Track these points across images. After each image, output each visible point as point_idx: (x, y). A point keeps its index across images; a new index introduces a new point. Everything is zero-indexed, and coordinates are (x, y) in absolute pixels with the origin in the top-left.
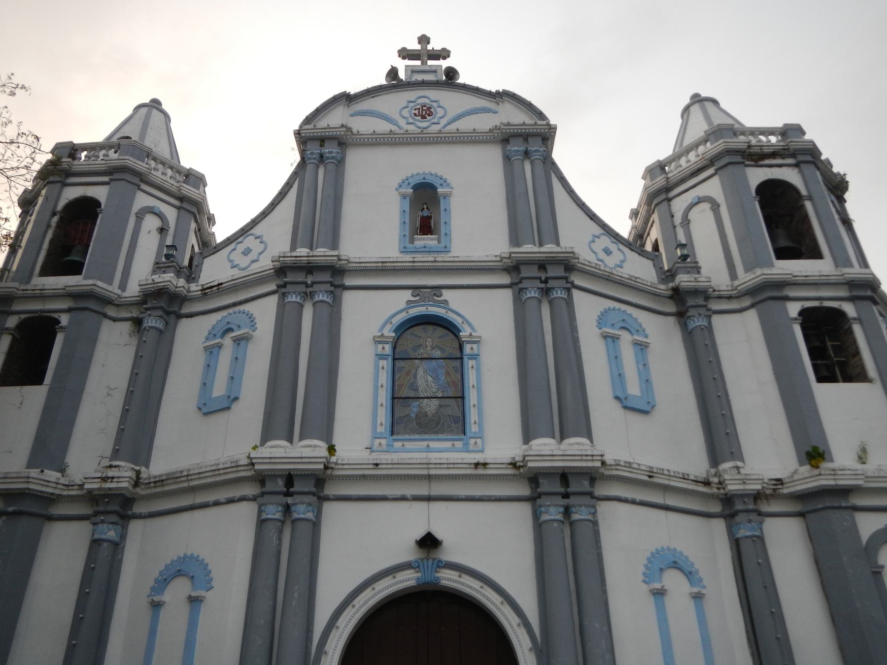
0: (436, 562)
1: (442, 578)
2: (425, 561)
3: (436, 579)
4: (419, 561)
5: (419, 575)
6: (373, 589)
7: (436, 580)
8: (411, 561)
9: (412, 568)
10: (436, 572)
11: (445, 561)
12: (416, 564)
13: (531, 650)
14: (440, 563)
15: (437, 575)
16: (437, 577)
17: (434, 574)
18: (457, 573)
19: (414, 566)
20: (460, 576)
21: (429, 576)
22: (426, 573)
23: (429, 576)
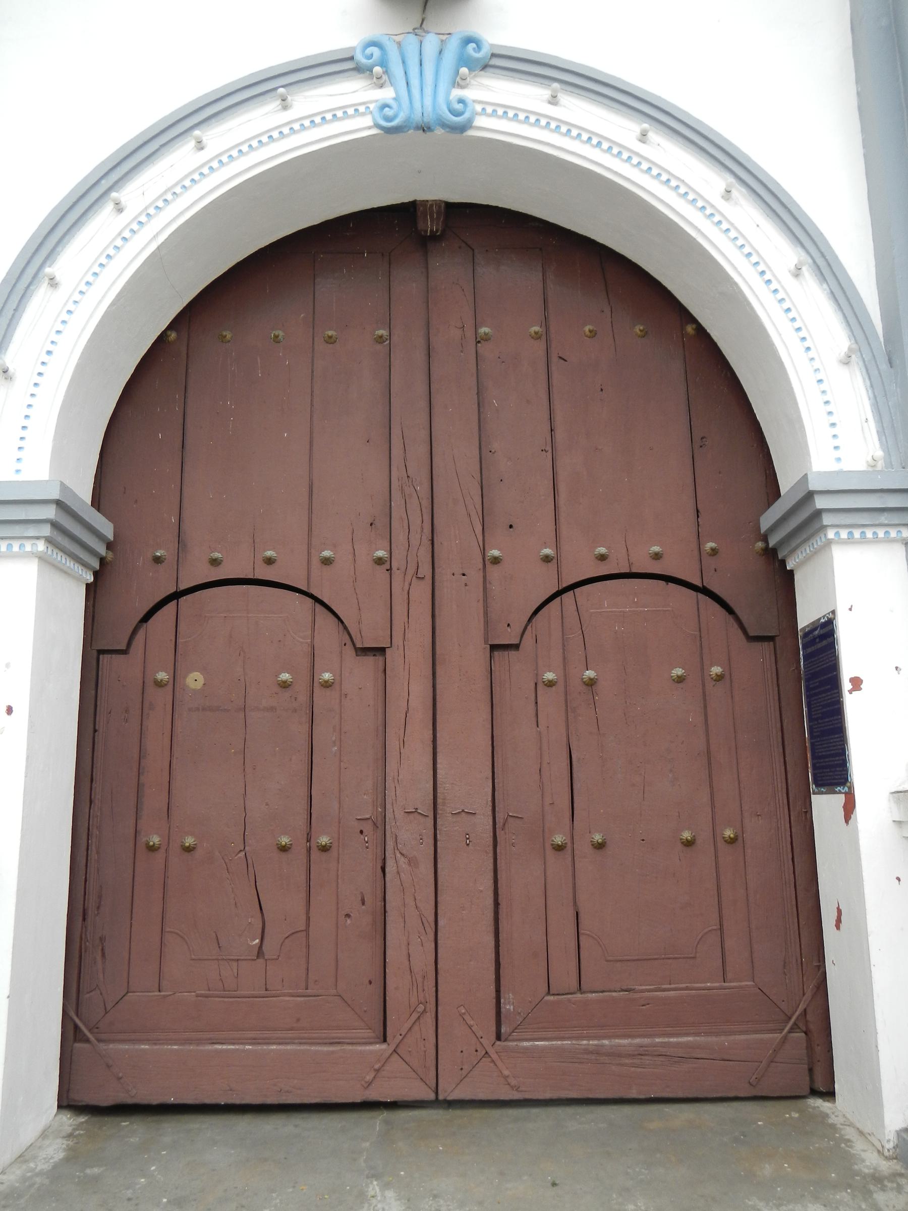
0: (453, 45)
1: (478, 108)
2: (411, 42)
3: (459, 107)
4: (385, 41)
5: (387, 94)
6: (200, 146)
7: (457, 114)
8: (353, 49)
9: (359, 69)
10: (457, 82)
11: (492, 46)
12: (375, 51)
13: (846, 361)
14: (472, 46)
15: (456, 93)
16: (461, 101)
17: (448, 93)
18: (545, 93)
19: (364, 61)
20: (553, 100)
21: (428, 90)
22: (415, 82)
23: (428, 90)
